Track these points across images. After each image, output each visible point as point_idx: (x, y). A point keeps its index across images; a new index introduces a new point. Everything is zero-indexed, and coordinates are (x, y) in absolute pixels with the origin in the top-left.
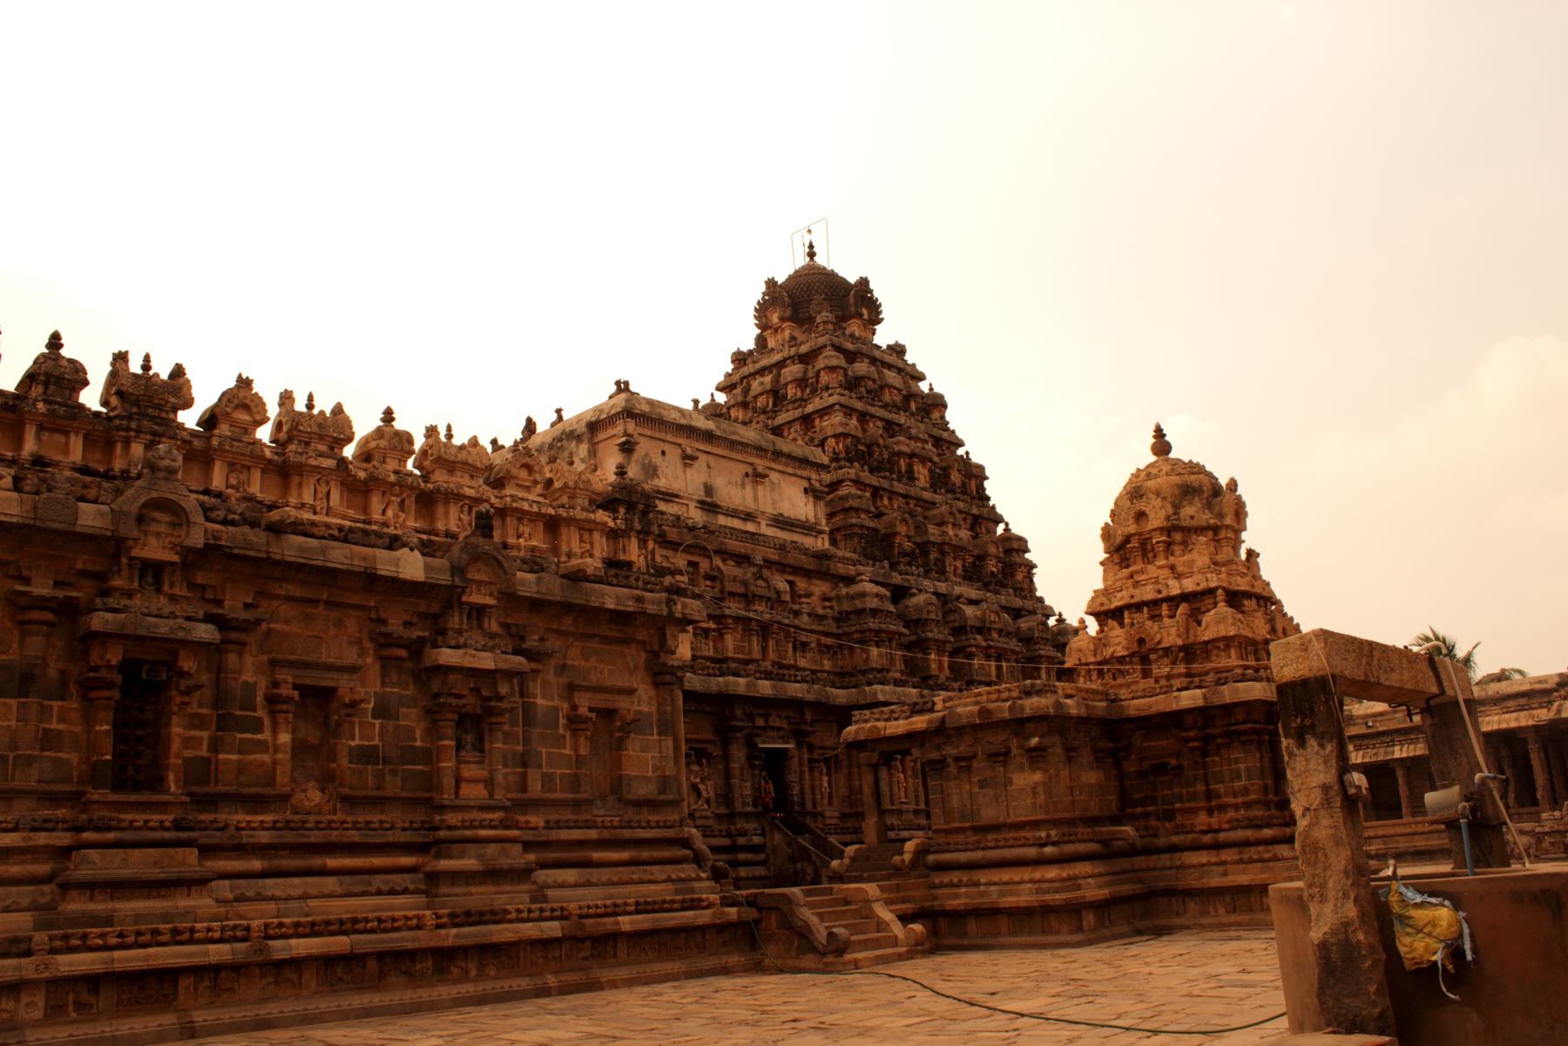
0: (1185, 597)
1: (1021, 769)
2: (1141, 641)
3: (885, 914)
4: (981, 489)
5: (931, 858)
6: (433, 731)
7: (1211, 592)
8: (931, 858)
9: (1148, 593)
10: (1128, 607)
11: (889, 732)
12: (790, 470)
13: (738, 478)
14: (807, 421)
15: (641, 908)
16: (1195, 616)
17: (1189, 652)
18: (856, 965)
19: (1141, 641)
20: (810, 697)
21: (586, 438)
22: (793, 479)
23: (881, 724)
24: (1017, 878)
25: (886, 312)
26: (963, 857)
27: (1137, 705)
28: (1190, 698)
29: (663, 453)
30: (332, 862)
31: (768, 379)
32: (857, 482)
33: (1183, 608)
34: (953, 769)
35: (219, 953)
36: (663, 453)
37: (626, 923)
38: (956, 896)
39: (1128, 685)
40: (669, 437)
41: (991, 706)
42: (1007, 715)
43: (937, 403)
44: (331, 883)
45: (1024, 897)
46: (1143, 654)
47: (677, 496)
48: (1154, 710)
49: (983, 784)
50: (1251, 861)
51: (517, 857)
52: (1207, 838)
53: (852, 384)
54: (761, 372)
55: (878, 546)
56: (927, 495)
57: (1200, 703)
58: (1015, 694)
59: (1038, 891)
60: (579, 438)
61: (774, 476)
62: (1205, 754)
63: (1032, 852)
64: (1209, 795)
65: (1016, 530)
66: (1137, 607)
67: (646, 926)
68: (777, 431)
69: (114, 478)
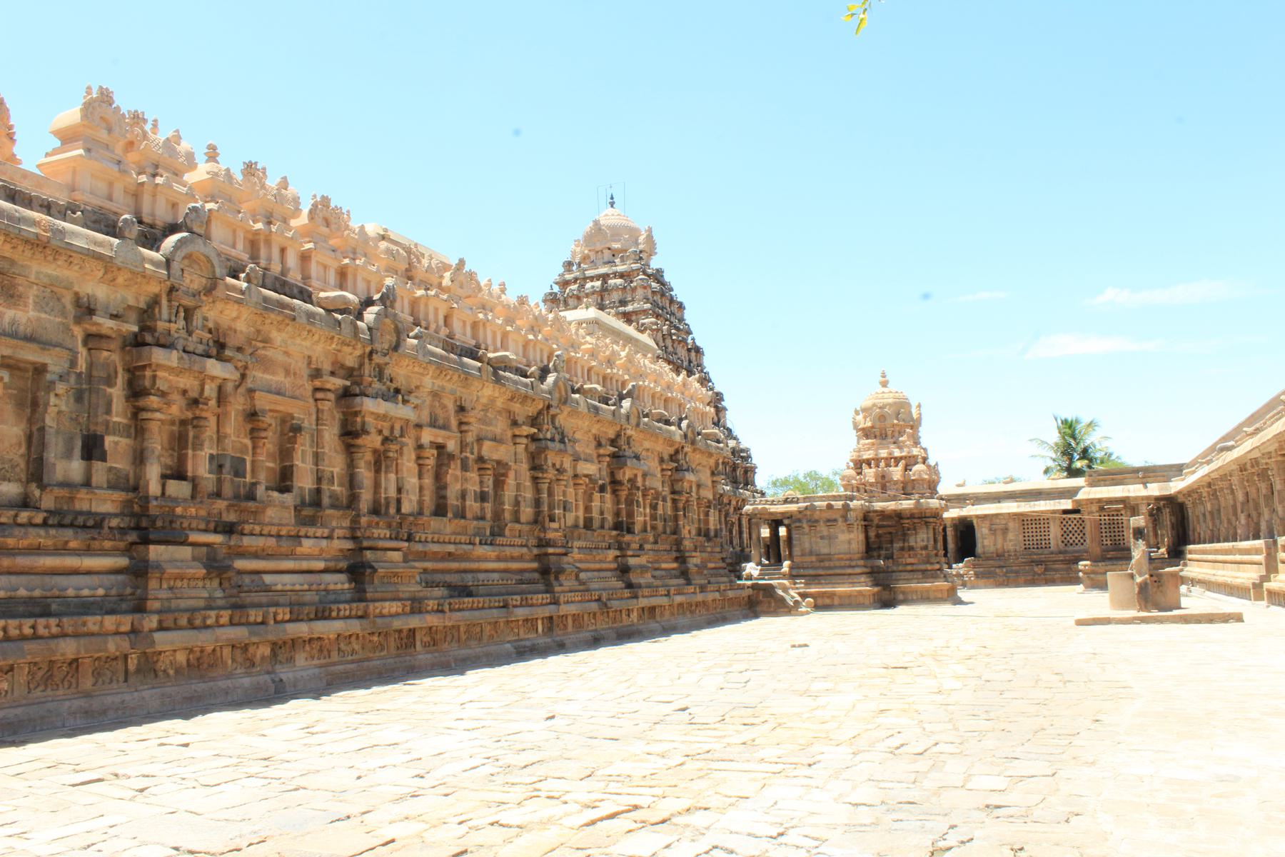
0: (901, 458)
1: (843, 532)
9: (883, 453)
16: (907, 468)
18: (802, 614)
19: (883, 477)
27: (878, 505)
28: (907, 504)
31: (598, 284)
34: (807, 529)
43: (681, 306)
46: (884, 482)
49: (822, 538)
52: (909, 568)
54: (592, 279)
64: (911, 548)
66: (878, 460)
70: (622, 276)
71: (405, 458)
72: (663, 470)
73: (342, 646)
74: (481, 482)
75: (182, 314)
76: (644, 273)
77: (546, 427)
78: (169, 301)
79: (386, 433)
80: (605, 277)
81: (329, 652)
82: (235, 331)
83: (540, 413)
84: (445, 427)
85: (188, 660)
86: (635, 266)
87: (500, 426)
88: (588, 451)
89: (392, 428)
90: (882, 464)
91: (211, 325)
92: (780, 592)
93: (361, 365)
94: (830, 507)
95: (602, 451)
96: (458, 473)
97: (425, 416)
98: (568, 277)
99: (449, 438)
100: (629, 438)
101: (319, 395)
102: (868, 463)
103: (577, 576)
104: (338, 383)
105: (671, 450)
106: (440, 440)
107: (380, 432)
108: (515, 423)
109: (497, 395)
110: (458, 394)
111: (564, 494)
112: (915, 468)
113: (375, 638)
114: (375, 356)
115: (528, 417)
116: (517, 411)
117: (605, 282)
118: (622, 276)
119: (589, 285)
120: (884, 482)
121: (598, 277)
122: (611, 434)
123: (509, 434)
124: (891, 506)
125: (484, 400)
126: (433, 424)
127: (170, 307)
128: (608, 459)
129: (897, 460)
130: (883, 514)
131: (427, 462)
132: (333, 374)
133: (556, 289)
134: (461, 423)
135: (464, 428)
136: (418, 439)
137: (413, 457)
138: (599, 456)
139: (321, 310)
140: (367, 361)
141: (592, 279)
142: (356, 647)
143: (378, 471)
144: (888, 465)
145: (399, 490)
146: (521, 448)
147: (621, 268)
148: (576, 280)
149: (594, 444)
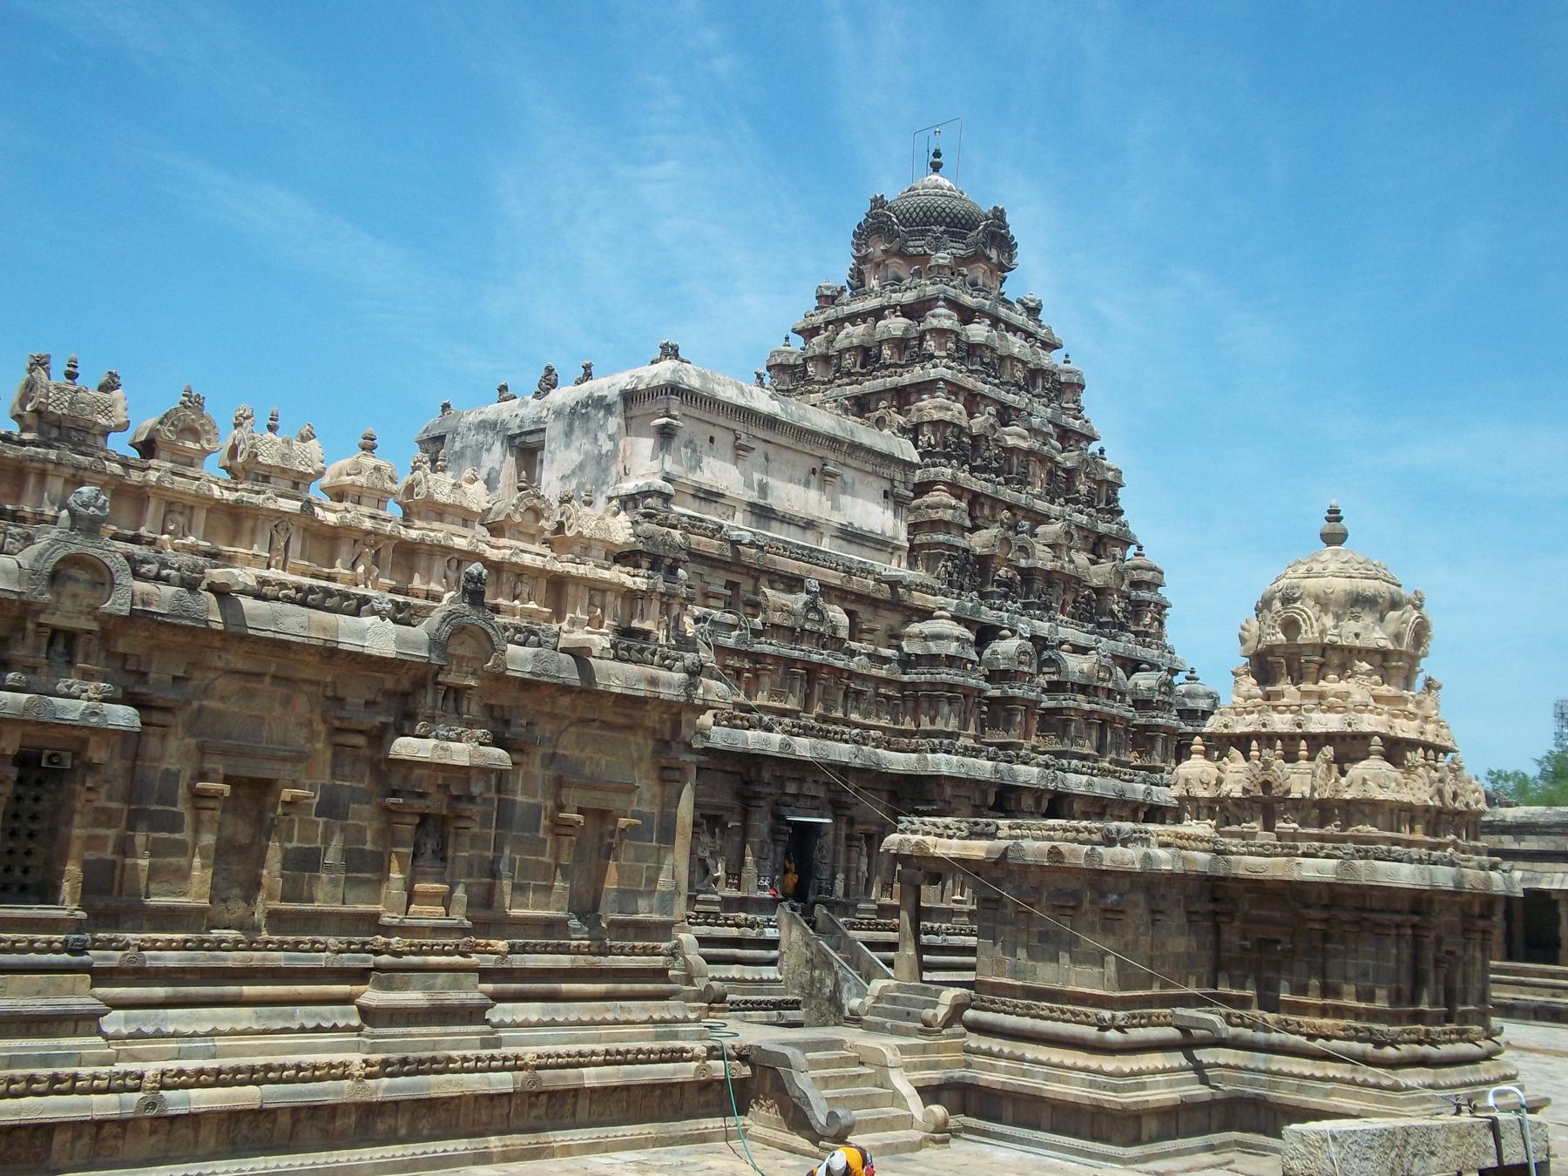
0: (1329, 738)
2: (1266, 785)
3: (903, 1083)
4: (1112, 499)
5: (970, 1014)
6: (388, 836)
7: (1366, 737)
8: (970, 1014)
9: (1281, 723)
10: (1257, 736)
11: (939, 852)
12: (869, 468)
13: (801, 474)
14: (903, 397)
15: (611, 1059)
17: (1323, 810)
20: (858, 762)
21: (620, 407)
22: (871, 478)
23: (930, 839)
24: (1068, 1062)
26: (1011, 1021)
27: (1248, 864)
29: (712, 440)
30: (248, 990)
31: (861, 328)
32: (954, 488)
33: (1328, 751)
35: (104, 1106)
36: (712, 440)
37: (592, 1077)
38: (993, 1068)
39: (1242, 836)
40: (722, 421)
41: (1064, 847)
42: (1082, 862)
44: (244, 1017)
45: (1072, 1090)
46: (1266, 804)
47: (722, 496)
50: (1365, 1084)
51: (472, 993)
53: (969, 352)
54: (853, 318)
55: (973, 572)
56: (1041, 505)
57: (1330, 877)
58: (1096, 837)
59: (1092, 1084)
60: (609, 409)
61: (848, 475)
62: (1326, 937)
63: (1091, 1032)
65: (1151, 557)
66: (1268, 739)
67: (614, 1082)
68: (861, 406)
69: (24, 520)
80: (878, 314)
102: (1242, 742)
112: (1357, 770)
124: (1274, 868)
129: (1317, 741)
144: (1290, 757)
148: (828, 323)
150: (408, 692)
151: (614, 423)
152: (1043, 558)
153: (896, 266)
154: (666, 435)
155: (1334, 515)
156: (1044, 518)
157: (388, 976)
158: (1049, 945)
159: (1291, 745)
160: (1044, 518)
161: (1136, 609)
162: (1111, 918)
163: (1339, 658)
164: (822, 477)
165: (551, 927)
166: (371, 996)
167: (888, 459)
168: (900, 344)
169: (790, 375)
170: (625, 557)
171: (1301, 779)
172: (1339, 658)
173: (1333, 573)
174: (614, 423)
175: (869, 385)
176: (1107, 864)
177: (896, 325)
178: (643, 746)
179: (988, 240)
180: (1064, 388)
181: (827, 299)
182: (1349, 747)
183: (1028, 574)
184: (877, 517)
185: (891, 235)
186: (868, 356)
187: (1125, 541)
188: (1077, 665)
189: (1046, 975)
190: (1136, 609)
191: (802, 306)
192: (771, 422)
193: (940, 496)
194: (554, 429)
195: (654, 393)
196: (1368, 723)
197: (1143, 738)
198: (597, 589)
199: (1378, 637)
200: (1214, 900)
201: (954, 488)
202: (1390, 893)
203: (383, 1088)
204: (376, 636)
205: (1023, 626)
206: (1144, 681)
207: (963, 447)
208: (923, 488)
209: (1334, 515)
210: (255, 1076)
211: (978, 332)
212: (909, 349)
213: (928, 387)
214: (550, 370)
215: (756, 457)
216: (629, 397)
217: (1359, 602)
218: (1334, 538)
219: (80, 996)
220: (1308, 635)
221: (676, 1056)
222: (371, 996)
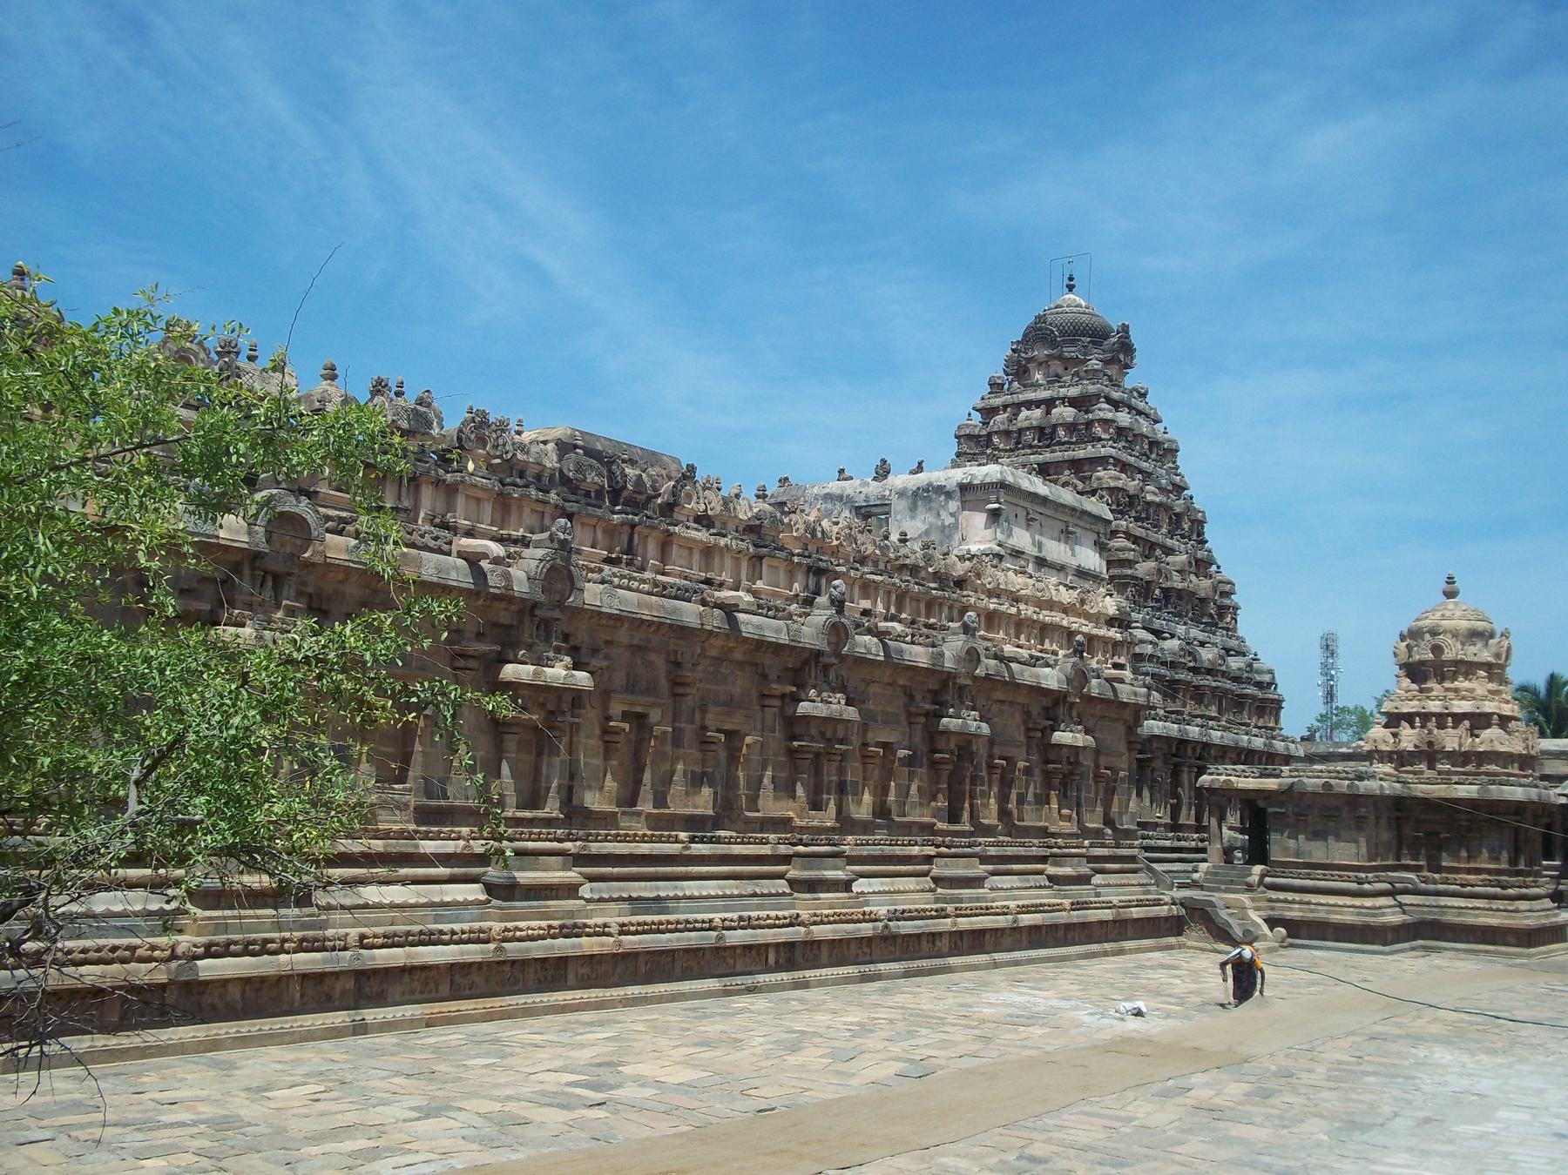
0: (1465, 716)
2: (1430, 744)
3: (1255, 917)
4: (1200, 534)
5: (1268, 880)
7: (1489, 716)
8: (1268, 880)
9: (1434, 706)
10: (1418, 714)
13: (1056, 535)
14: (1076, 465)
23: (1233, 778)
25: (1139, 358)
26: (1298, 882)
27: (1421, 790)
31: (1037, 413)
32: (1128, 535)
33: (1467, 723)
34: (1292, 820)
35: (1002, 922)
38: (1290, 909)
39: (1415, 773)
40: (1022, 503)
41: (1332, 781)
42: (1345, 790)
44: (1013, 881)
45: (1348, 918)
46: (1430, 754)
48: (1436, 795)
50: (1498, 910)
51: (1085, 869)
53: (1121, 432)
54: (1029, 404)
56: (1169, 542)
57: (1475, 796)
59: (1358, 914)
60: (949, 495)
62: (1469, 830)
63: (1354, 886)
65: (1226, 573)
66: (1426, 717)
68: (1044, 470)
70: (1072, 402)
71: (582, 735)
72: (1028, 729)
73: (457, 978)
74: (704, 760)
75: (270, 583)
76: (1109, 400)
77: (812, 681)
78: (253, 569)
79: (550, 707)
80: (1049, 404)
81: (437, 984)
82: (344, 594)
83: (806, 662)
84: (652, 690)
85: (243, 992)
86: (1092, 389)
87: (739, 684)
88: (889, 709)
89: (560, 700)
90: (1432, 724)
91: (310, 590)
92: (1223, 914)
93: (521, 622)
94: (1327, 785)
95: (913, 710)
96: (668, 749)
97: (619, 678)
98: (998, 401)
99: (653, 705)
100: (961, 688)
101: (461, 663)
102: (1409, 718)
103: (846, 886)
104: (484, 647)
105: (1047, 702)
106: (638, 709)
107: (542, 705)
108: (764, 676)
109: (732, 644)
110: (672, 647)
111: (841, 771)
112: (1486, 734)
113: (507, 968)
114: (537, 612)
115: (786, 669)
116: (767, 662)
117: (1048, 412)
118: (1072, 402)
119: (1024, 413)
120: (1430, 754)
121: (1037, 404)
122: (933, 684)
123: (754, 694)
124: (1438, 791)
125: (714, 653)
126: (631, 688)
127: (253, 577)
128: (923, 720)
129: (1458, 718)
130: (1427, 803)
131: (616, 738)
132: (480, 636)
133: (977, 417)
134: (675, 683)
135: (680, 690)
136: (605, 708)
137: (598, 731)
138: (909, 714)
139: (461, 562)
140: (527, 618)
141: (1029, 404)
142: (477, 979)
143: (539, 754)
144: (1441, 726)
145: (572, 777)
146: (771, 713)
147: (1073, 392)
148: (1005, 407)
149: (903, 700)
150: (1053, 707)
151: (954, 505)
152: (1177, 582)
153: (1057, 367)
154: (995, 515)
155: (1450, 580)
156: (1169, 551)
157: (1057, 859)
158: (1318, 835)
159: (1441, 719)
160: (1169, 551)
161: (1222, 610)
162: (1360, 824)
163: (1467, 668)
164: (1067, 535)
165: (1098, 833)
166: (1051, 870)
167: (1099, 519)
168: (1071, 427)
169: (974, 445)
170: (1111, 622)
171: (1451, 739)
172: (1467, 668)
173: (1456, 617)
174: (954, 505)
175: (1047, 456)
176: (1362, 791)
177: (1065, 413)
178: (1121, 729)
179: (1122, 351)
180: (1166, 452)
181: (996, 387)
182: (1479, 721)
183: (1165, 591)
184: (1091, 559)
185: (1053, 344)
186: (1045, 434)
187: (1210, 562)
188: (1207, 655)
189: (1317, 851)
190: (1222, 610)
191: (979, 392)
192: (1044, 501)
193: (1120, 542)
194: (899, 506)
195: (985, 487)
196: (1489, 707)
197: (1239, 702)
198: (1105, 641)
199: (1486, 656)
200: (1400, 809)
201: (1128, 535)
202: (1458, 801)
203: (1076, 916)
204: (1051, 678)
205: (1181, 630)
206: (1235, 663)
207: (1125, 503)
208: (1114, 534)
209: (1450, 580)
210: (1036, 909)
211: (1124, 418)
212: (1082, 432)
213: (1102, 461)
214: (884, 461)
215: (1036, 525)
216: (964, 488)
217: (1475, 635)
218: (1450, 594)
219: (981, 870)
220: (1448, 655)
221: (1157, 903)
222: (1051, 870)
